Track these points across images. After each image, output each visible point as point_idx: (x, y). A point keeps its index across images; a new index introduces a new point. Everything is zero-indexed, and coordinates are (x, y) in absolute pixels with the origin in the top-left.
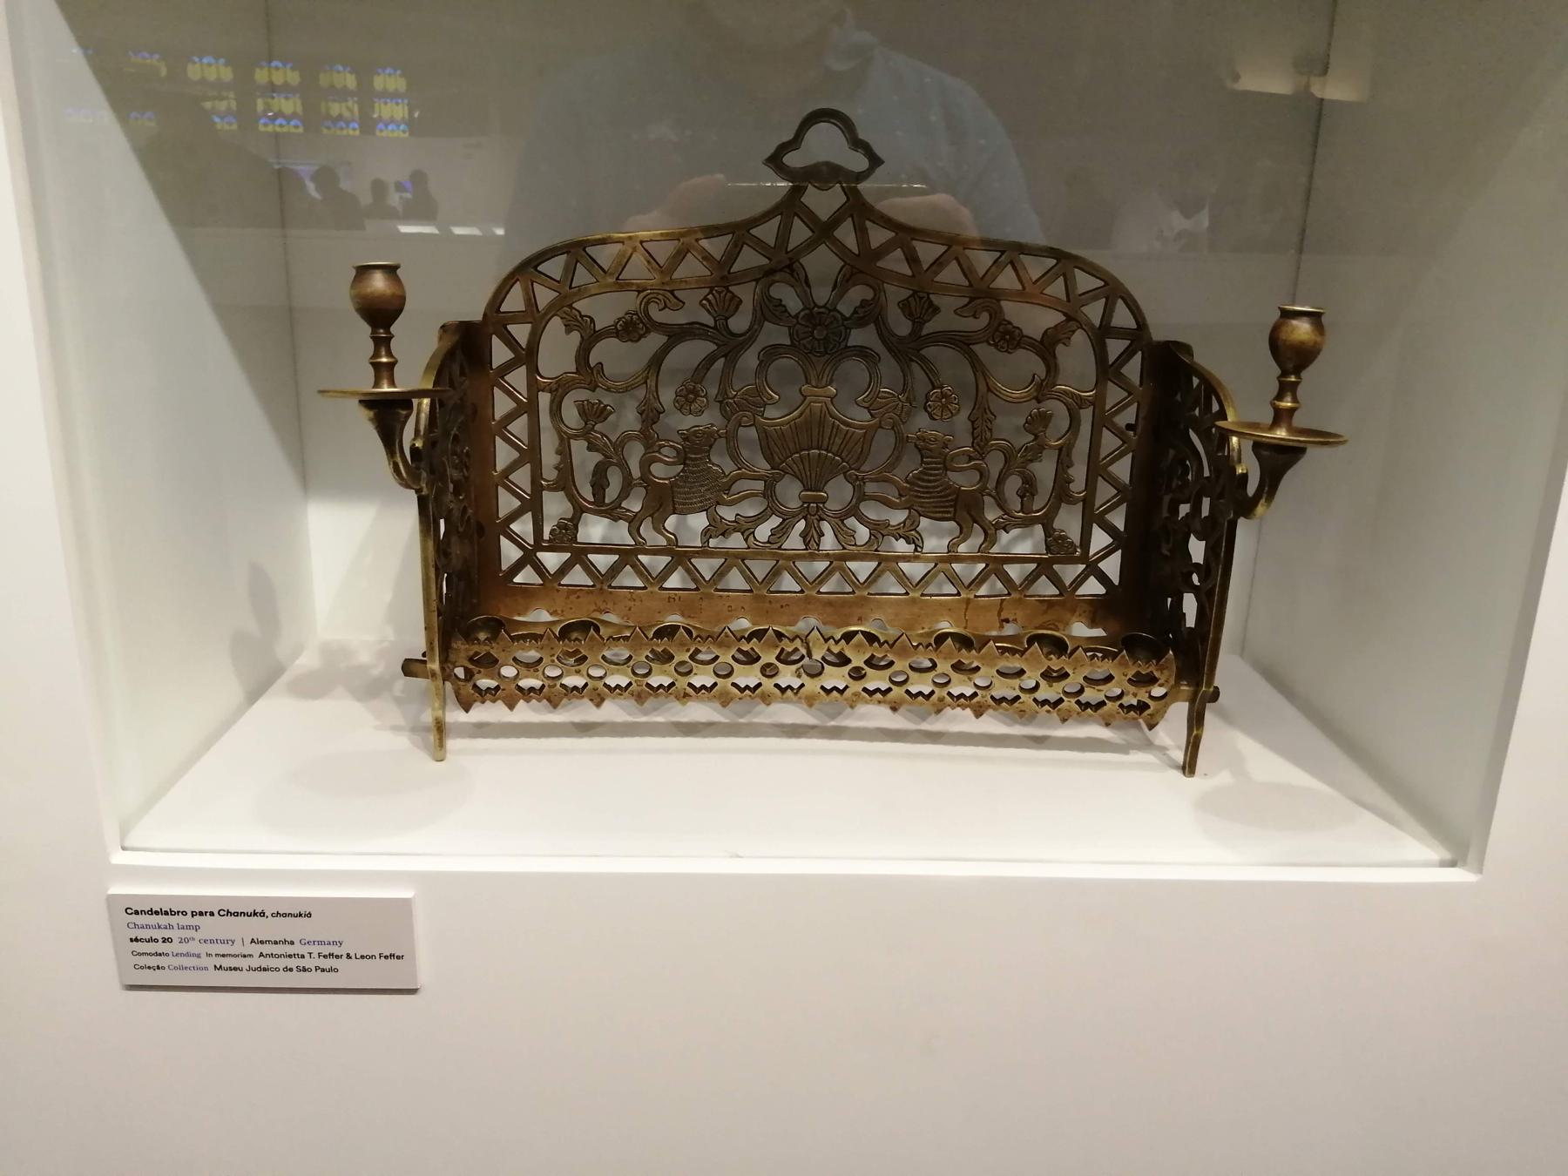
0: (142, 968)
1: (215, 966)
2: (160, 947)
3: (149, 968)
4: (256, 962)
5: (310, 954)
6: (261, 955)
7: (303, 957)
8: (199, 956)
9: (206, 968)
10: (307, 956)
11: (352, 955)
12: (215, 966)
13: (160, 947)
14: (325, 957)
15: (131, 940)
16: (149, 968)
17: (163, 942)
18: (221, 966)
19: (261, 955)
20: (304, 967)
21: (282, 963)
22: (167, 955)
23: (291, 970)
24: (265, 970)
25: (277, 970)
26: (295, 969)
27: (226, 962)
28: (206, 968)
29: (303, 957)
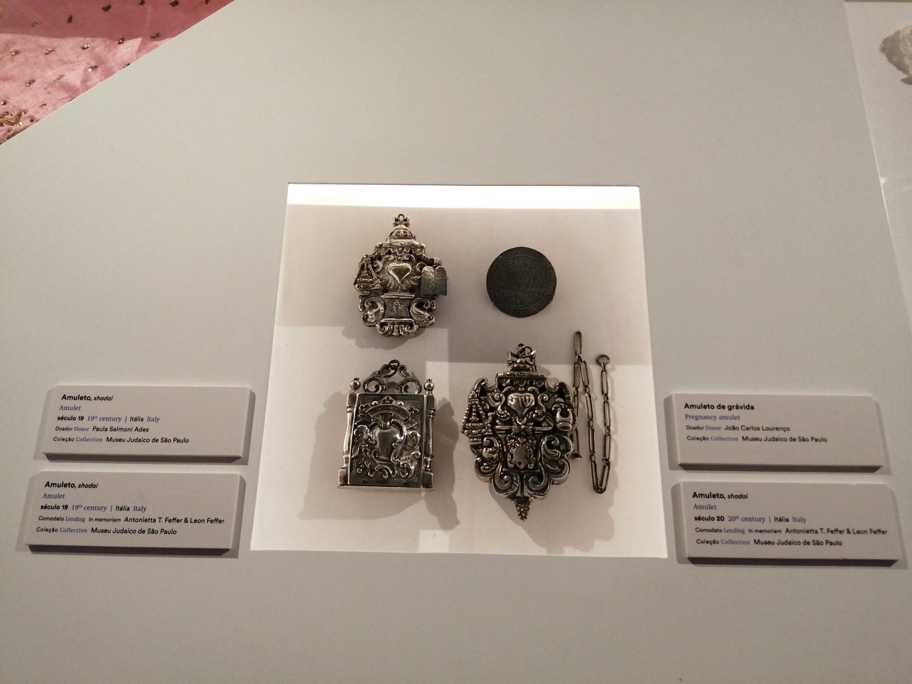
0: (703, 542)
1: (755, 541)
2: (715, 525)
3: (707, 542)
4: (784, 537)
5: (822, 529)
6: (787, 531)
7: (816, 532)
8: (743, 532)
9: (748, 543)
10: (819, 531)
11: (851, 530)
12: (755, 541)
13: (715, 525)
14: (832, 532)
15: (696, 519)
16: (707, 542)
17: (718, 520)
18: (759, 540)
19: (787, 531)
20: (818, 541)
21: (802, 537)
22: (721, 531)
23: (808, 543)
24: (790, 543)
25: (799, 543)
26: (811, 543)
27: (764, 537)
28: (748, 543)
29: (816, 532)
